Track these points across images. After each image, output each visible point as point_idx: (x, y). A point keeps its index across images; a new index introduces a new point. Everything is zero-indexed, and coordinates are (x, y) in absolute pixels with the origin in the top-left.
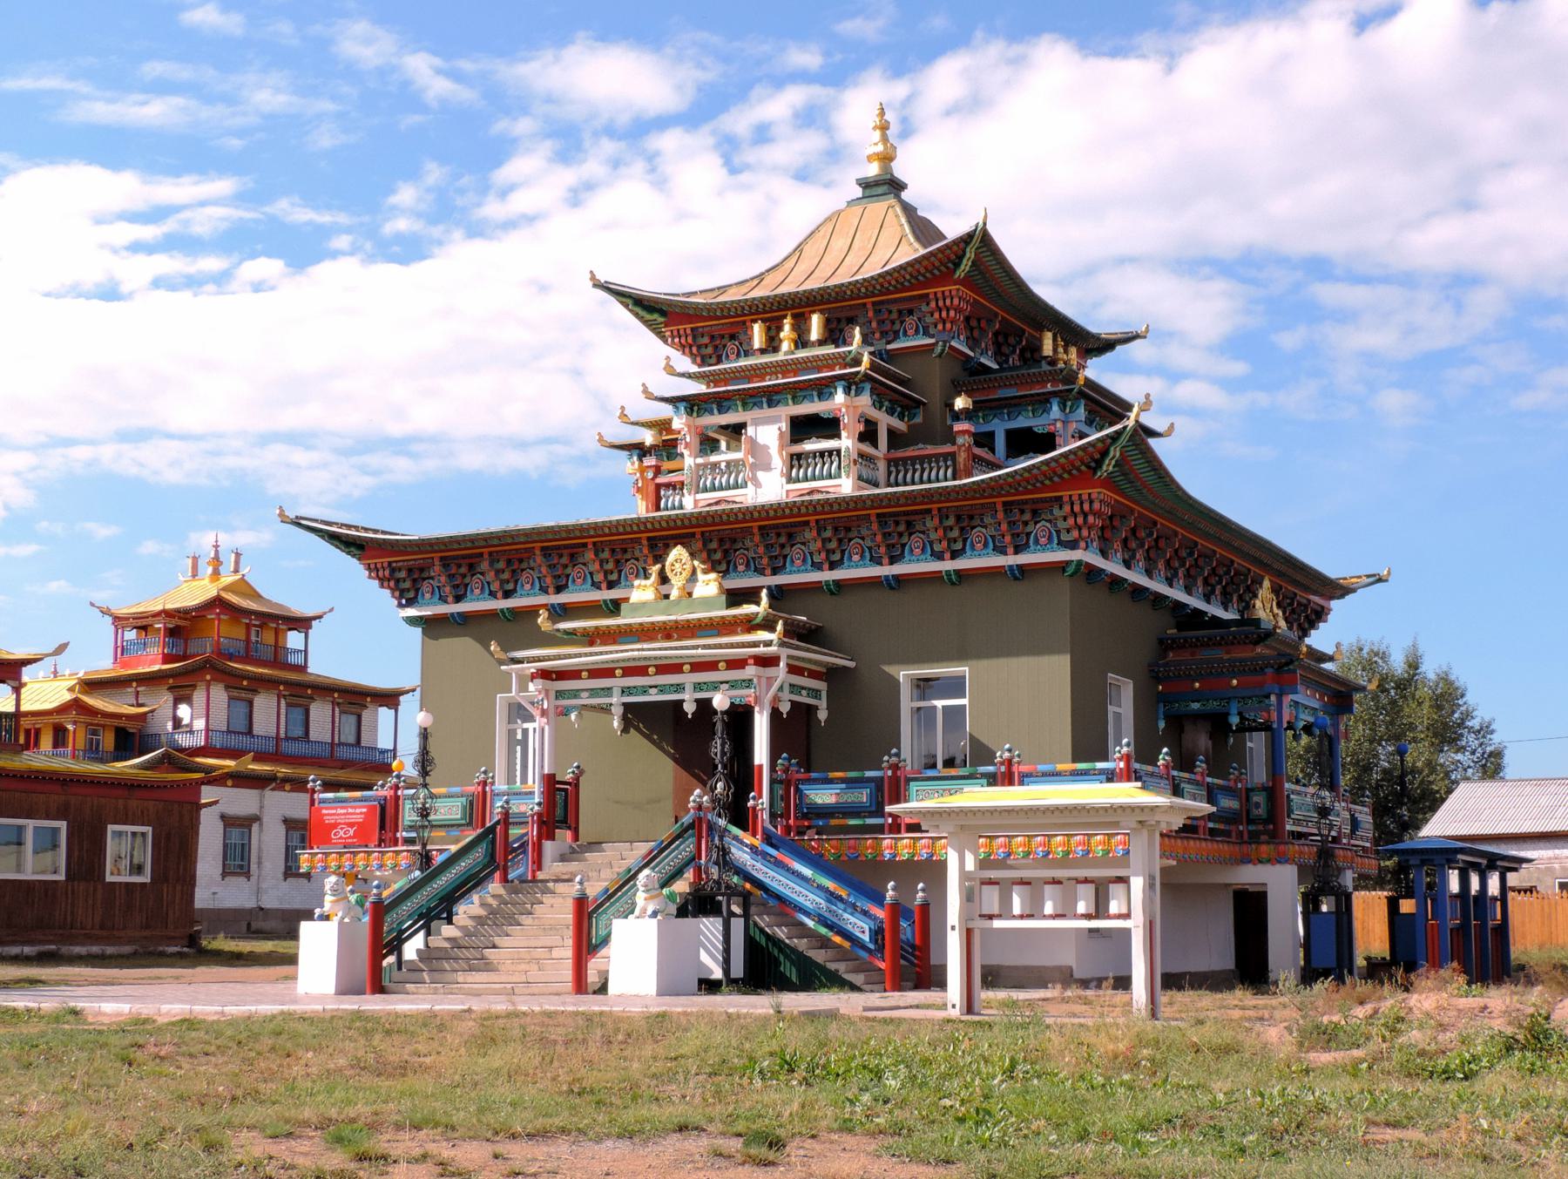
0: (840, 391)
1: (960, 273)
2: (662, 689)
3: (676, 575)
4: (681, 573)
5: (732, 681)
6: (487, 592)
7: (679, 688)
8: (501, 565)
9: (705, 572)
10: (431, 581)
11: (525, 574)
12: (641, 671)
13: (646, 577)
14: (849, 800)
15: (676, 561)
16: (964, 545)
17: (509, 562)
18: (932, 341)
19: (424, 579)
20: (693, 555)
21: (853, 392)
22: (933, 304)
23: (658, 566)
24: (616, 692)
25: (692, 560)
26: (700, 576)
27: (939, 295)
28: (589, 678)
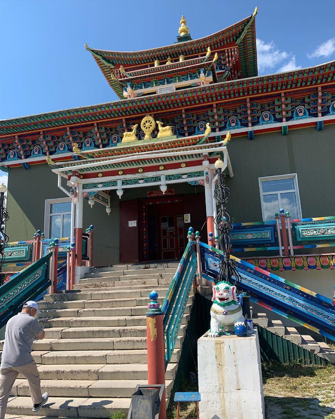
0: (202, 72)
1: (238, 41)
2: (146, 180)
3: (147, 128)
4: (149, 128)
5: (189, 173)
6: (41, 152)
7: (158, 179)
8: (49, 138)
9: (163, 126)
10: (14, 150)
11: (60, 144)
12: (135, 171)
13: (130, 130)
14: (259, 237)
15: (146, 122)
16: (293, 114)
17: (53, 138)
18: (224, 71)
19: (10, 149)
20: (156, 119)
21: (206, 74)
22: (227, 54)
23: (136, 125)
24: (119, 183)
25: (155, 121)
26: (160, 128)
27: (229, 50)
28: (102, 176)
